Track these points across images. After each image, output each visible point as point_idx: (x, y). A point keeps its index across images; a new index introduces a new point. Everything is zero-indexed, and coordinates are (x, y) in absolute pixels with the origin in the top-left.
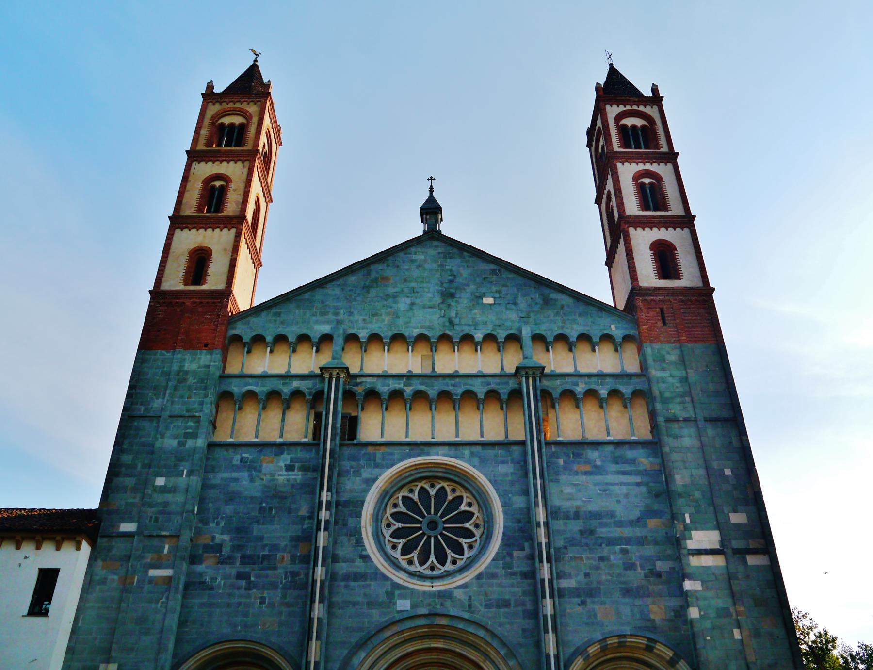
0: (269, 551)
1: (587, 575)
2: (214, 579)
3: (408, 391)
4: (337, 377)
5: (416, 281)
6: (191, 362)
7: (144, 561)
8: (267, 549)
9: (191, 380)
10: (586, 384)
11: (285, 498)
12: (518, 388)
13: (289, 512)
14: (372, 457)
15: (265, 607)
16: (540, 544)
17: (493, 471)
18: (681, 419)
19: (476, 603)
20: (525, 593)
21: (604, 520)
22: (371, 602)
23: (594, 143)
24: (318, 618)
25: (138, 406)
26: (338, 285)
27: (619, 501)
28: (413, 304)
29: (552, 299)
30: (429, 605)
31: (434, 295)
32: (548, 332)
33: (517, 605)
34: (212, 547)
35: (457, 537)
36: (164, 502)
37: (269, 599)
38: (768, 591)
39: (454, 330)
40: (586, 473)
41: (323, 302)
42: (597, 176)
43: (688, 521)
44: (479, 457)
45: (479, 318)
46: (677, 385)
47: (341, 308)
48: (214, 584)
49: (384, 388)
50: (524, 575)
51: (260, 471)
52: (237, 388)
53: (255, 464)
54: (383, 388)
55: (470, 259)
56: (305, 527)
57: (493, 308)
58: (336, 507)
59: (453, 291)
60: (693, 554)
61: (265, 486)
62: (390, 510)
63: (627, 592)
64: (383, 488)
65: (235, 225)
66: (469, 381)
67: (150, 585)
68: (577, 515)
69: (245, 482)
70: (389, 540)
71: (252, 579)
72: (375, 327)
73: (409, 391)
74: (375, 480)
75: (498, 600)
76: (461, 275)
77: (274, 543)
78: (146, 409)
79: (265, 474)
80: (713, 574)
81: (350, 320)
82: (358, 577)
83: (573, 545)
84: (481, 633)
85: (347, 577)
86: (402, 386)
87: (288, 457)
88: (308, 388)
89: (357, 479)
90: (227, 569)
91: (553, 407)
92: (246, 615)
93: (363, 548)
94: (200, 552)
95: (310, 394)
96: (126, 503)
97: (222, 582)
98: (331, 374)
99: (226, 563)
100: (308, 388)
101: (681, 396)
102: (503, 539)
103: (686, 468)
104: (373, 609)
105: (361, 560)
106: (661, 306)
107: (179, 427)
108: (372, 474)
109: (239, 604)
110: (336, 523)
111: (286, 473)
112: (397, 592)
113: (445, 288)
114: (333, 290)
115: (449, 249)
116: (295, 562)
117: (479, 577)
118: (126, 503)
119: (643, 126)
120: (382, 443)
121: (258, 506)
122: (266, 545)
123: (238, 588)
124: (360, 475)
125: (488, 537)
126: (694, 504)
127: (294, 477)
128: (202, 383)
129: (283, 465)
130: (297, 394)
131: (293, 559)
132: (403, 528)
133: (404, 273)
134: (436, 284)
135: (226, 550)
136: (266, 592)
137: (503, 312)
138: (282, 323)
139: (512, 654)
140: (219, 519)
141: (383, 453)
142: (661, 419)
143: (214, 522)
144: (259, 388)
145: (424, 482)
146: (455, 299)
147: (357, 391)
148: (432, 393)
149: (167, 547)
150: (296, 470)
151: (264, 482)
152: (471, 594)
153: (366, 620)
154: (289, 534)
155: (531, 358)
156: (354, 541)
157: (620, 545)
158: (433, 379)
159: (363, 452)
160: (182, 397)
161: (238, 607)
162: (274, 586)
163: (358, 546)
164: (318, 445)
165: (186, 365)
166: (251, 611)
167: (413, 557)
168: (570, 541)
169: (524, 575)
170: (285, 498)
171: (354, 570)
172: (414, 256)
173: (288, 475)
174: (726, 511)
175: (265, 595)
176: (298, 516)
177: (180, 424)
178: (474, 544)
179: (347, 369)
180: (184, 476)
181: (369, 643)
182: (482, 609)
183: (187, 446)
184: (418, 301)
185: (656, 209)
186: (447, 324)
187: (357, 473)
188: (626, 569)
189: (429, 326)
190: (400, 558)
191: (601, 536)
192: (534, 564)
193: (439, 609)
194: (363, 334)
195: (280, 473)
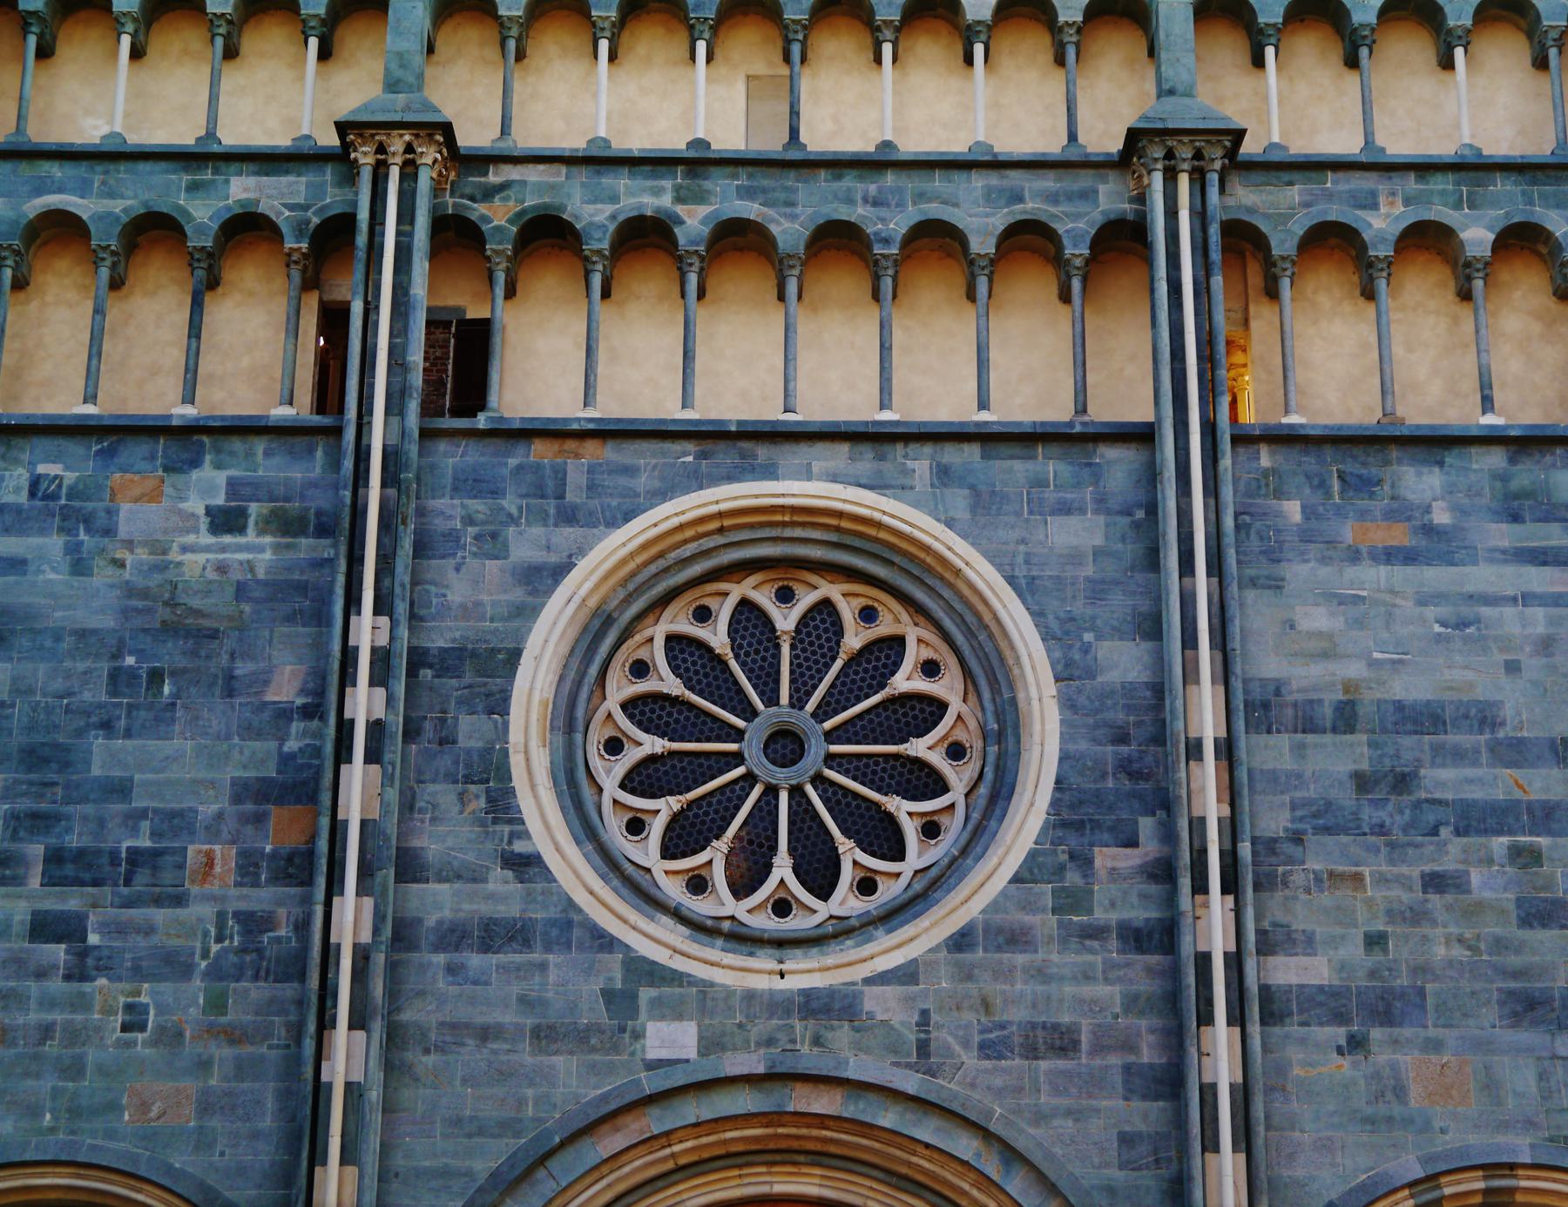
0: (154, 834)
1: (1375, 941)
3: (689, 221)
4: (406, 163)
8: (145, 826)
11: (214, 635)
12: (1130, 217)
13: (230, 692)
14: (550, 484)
15: (144, 1043)
16: (1197, 825)
17: (1023, 541)
19: (942, 1036)
20: (1131, 1003)
21: (1453, 738)
22: (551, 1027)
24: (349, 1086)
27: (1512, 668)
30: (770, 1042)
33: (1098, 1049)
35: (879, 790)
40: (1390, 556)
44: (972, 487)
50: (1135, 938)
51: (109, 532)
53: (90, 505)
54: (590, 208)
56: (292, 745)
58: (412, 672)
61: (130, 591)
62: (620, 688)
64: (593, 603)
66: (938, 182)
68: (1346, 718)
69: (54, 575)
70: (615, 802)
71: (93, 939)
73: (694, 222)
74: (560, 571)
75: (1034, 1026)
77: (175, 805)
79: (130, 544)
83: (1327, 830)
84: (965, 1146)
85: (454, 937)
86: (666, 201)
87: (221, 477)
88: (291, 207)
89: (492, 566)
91: (1272, 293)
92: (75, 1069)
93: (519, 828)
95: (300, 229)
98: (381, 149)
100: (291, 207)
102: (1055, 803)
104: (556, 1053)
105: (509, 874)
109: (46, 1031)
110: (411, 732)
111: (207, 539)
112: (646, 994)
116: (257, 875)
117: (961, 941)
120: (591, 426)
121: (104, 666)
122: (143, 814)
123: (41, 974)
124: (501, 553)
129: (201, 511)
131: (248, 868)
141: (591, 470)
145: (752, 580)
147: (488, 220)
148: (789, 231)
150: (251, 530)
151: (127, 576)
153: (530, 1092)
154: (233, 772)
155: (1189, 94)
156: (482, 803)
157: (1511, 833)
158: (792, 174)
159: (513, 462)
161: (42, 1042)
162: (175, 965)
163: (495, 821)
164: (337, 431)
166: (92, 1055)
167: (710, 862)
168: (1315, 816)
169: (1135, 938)
171: (486, 909)
173: (224, 549)
175: (144, 999)
176: (266, 704)
178: (944, 820)
179: (447, 129)
181: (541, 1173)
182: (970, 1060)
187: (492, 542)
188: (1526, 922)
190: (659, 866)
191: (1437, 795)
192: (1171, 900)
193: (809, 1059)
195: (190, 539)
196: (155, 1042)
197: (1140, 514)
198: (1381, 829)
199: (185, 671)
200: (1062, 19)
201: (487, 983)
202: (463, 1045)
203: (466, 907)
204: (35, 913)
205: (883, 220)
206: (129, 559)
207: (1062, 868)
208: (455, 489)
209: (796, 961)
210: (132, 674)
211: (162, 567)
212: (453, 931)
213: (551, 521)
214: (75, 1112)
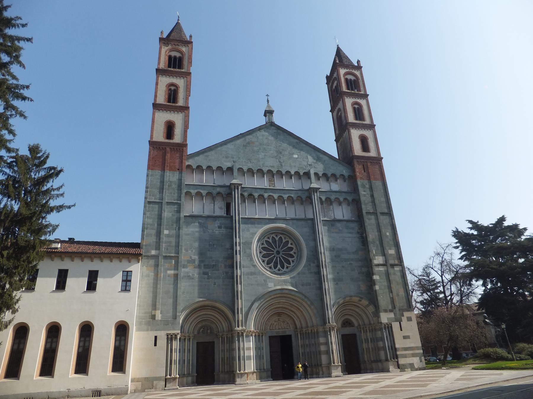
1: (338, 273)
5: (266, 145)
8: (214, 262)
10: (335, 195)
28: (265, 155)
35: (288, 257)
43: (374, 253)
45: (292, 164)
50: (316, 273)
55: (287, 136)
56: (229, 253)
71: (210, 274)
72: (250, 166)
74: (256, 233)
79: (210, 230)
82: (252, 274)
85: (248, 274)
87: (219, 222)
88: (224, 192)
89: (248, 232)
94: (186, 263)
103: (373, 232)
105: (253, 267)
111: (218, 229)
114: (230, 146)
117: (299, 274)
123: (204, 279)
125: (300, 258)
127: (222, 231)
129: (217, 226)
130: (219, 193)
131: (226, 266)
132: (267, 253)
134: (274, 147)
139: (312, 303)
145: (274, 234)
146: (282, 155)
156: (249, 259)
169: (316, 273)
175: (215, 281)
178: (294, 260)
184: (267, 154)
186: (280, 166)
194: (245, 169)
206: (210, 232)
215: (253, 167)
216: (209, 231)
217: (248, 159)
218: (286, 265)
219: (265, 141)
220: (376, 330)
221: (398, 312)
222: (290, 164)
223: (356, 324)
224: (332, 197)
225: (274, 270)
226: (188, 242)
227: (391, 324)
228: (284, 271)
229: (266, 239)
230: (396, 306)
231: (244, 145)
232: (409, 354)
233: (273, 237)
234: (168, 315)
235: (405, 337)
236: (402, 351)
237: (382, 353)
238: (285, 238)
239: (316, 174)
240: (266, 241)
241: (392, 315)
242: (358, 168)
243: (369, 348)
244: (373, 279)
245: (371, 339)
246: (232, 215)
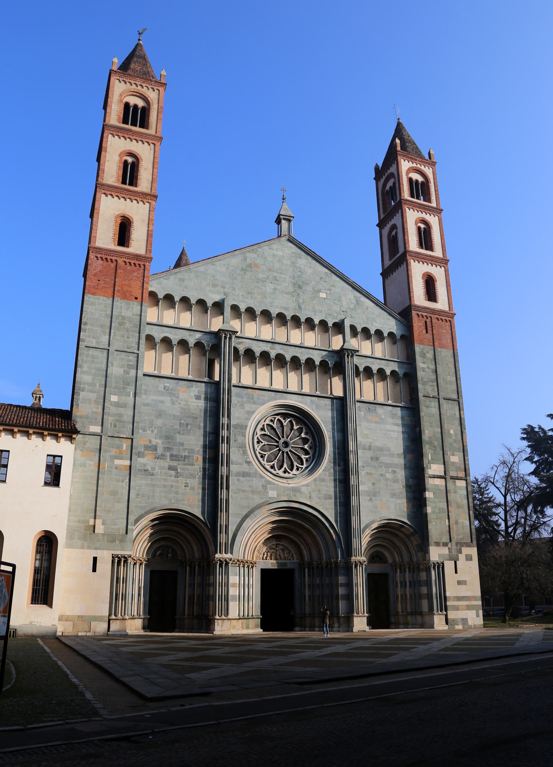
0: (188, 453)
1: (373, 484)
2: (153, 469)
5: (277, 272)
6: (126, 310)
7: (111, 453)
9: (128, 325)
11: (197, 418)
18: (432, 396)
22: (254, 491)
23: (382, 180)
25: (91, 339)
26: (224, 265)
28: (275, 289)
29: (361, 301)
30: (288, 495)
31: (289, 285)
32: (358, 325)
34: (150, 447)
36: (119, 414)
37: (191, 484)
38: (464, 500)
39: (301, 313)
40: (376, 422)
41: (213, 276)
42: (381, 206)
43: (430, 458)
46: (431, 374)
47: (227, 283)
48: (154, 472)
49: (258, 349)
51: (178, 397)
52: (158, 334)
53: (174, 392)
54: (256, 348)
56: (210, 439)
57: (325, 301)
59: (301, 284)
60: (429, 477)
61: (182, 409)
63: (393, 495)
65: (149, 201)
67: (116, 470)
71: (179, 471)
74: (253, 412)
76: (307, 273)
78: (97, 342)
80: (440, 489)
81: (233, 294)
82: (245, 474)
85: (238, 474)
87: (197, 390)
88: (207, 341)
89: (242, 410)
90: (162, 463)
92: (177, 493)
94: (143, 450)
95: (208, 345)
96: (92, 411)
97: (159, 471)
99: (161, 459)
101: (432, 382)
102: (329, 458)
104: (255, 495)
106: (426, 320)
107: (123, 359)
108: (251, 408)
109: (172, 486)
111: (196, 401)
112: (269, 486)
113: (296, 281)
115: (299, 251)
117: (315, 480)
118: (92, 411)
119: (422, 182)
120: (258, 388)
121: (178, 422)
122: (186, 449)
123: (170, 476)
124: (243, 408)
126: (433, 448)
128: (137, 328)
132: (267, 444)
133: (269, 263)
134: (290, 277)
135: (160, 451)
136: (188, 479)
137: (331, 305)
138: (186, 287)
140: (153, 428)
142: (421, 395)
143: (150, 430)
144: (175, 337)
146: (302, 290)
147: (239, 347)
149: (125, 445)
151: (181, 406)
152: (311, 490)
158: (288, 346)
159: (245, 392)
160: (123, 337)
162: (193, 476)
163: (244, 455)
165: (123, 312)
170: (197, 418)
172: (276, 252)
173: (198, 403)
174: (449, 455)
175: (188, 482)
177: (124, 357)
180: (131, 397)
182: (316, 499)
183: (130, 375)
184: (278, 287)
185: (427, 249)
186: (297, 308)
187: (242, 406)
188: (394, 482)
189: (286, 307)
196: (190, 489)
197: (341, 412)
198: (374, 466)
199: (192, 424)
200: (329, 325)
201: (243, 483)
202: (240, 493)
203: (240, 469)
204: (169, 465)
205: (302, 357)
207: (330, 469)
208: (236, 396)
209: (290, 481)
210: (183, 424)
211: (187, 405)
212: (238, 473)
213: (252, 403)
214: (177, 500)
215: (255, 306)
216: (180, 402)
217: (248, 292)
218: (297, 466)
219: (277, 265)
220: (419, 570)
221: (454, 547)
222: (314, 307)
223: (390, 561)
224: (373, 366)
225: (278, 471)
226: (146, 417)
227: (443, 564)
228: (293, 474)
229: (268, 422)
230: (452, 539)
231: (242, 267)
232: (462, 605)
233: (278, 420)
234: (113, 527)
235: (459, 583)
236: (454, 601)
237: (425, 603)
238: (297, 424)
239: (353, 328)
240: (267, 424)
241: (445, 551)
242: (417, 324)
243: (406, 595)
244: (424, 497)
245: (410, 582)
246: (217, 378)
